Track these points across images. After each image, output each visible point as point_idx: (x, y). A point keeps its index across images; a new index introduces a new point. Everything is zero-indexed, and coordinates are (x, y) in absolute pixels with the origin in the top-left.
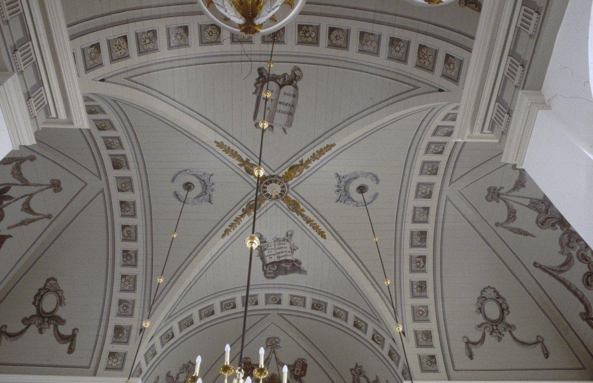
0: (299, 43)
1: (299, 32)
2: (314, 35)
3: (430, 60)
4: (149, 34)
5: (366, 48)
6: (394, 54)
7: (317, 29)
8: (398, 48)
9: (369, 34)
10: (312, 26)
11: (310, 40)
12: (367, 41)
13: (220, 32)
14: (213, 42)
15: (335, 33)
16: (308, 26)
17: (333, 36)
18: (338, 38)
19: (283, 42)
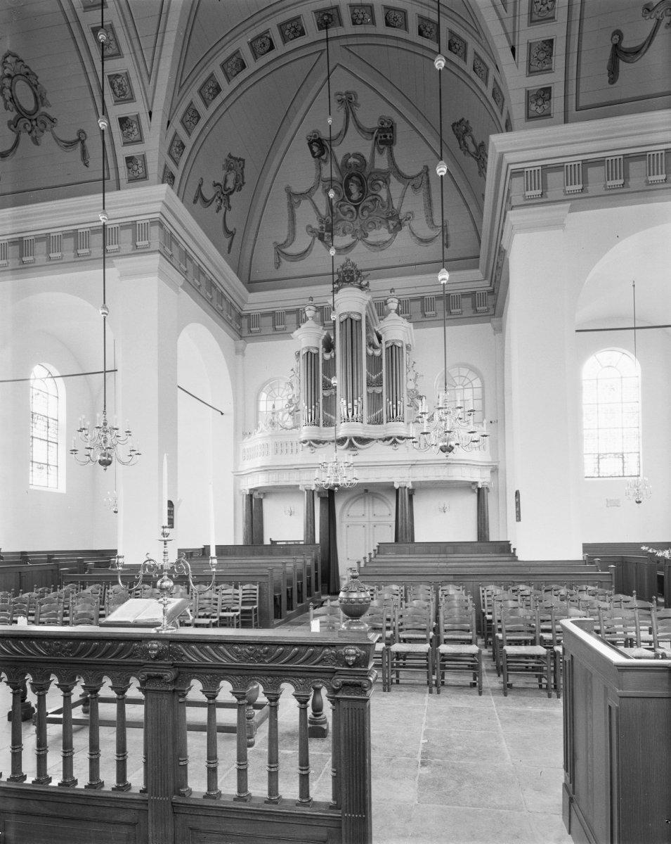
0: (299, 18)
1: (303, 28)
2: (287, 33)
3: (188, 123)
4: (455, 51)
5: (235, 59)
6: (210, 84)
7: (285, 41)
8: (211, 91)
9: (238, 73)
10: (291, 40)
11: (289, 26)
12: (237, 65)
13: (386, 18)
14: (392, 9)
15: (267, 47)
16: (295, 37)
17: (268, 43)
18: (262, 45)
19: (316, 12)
